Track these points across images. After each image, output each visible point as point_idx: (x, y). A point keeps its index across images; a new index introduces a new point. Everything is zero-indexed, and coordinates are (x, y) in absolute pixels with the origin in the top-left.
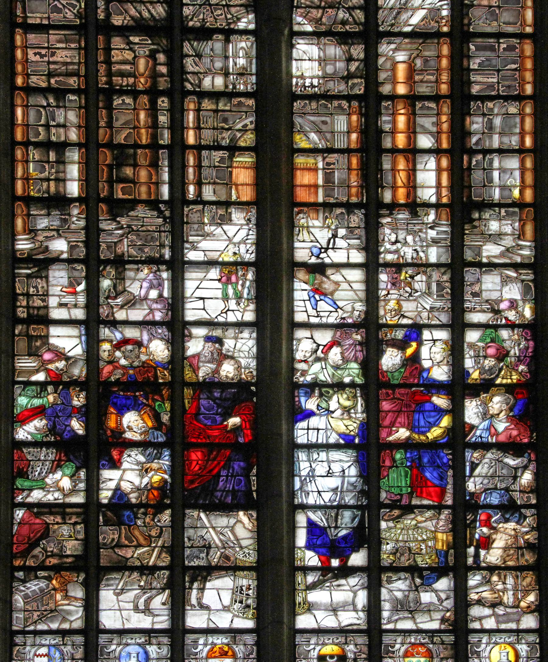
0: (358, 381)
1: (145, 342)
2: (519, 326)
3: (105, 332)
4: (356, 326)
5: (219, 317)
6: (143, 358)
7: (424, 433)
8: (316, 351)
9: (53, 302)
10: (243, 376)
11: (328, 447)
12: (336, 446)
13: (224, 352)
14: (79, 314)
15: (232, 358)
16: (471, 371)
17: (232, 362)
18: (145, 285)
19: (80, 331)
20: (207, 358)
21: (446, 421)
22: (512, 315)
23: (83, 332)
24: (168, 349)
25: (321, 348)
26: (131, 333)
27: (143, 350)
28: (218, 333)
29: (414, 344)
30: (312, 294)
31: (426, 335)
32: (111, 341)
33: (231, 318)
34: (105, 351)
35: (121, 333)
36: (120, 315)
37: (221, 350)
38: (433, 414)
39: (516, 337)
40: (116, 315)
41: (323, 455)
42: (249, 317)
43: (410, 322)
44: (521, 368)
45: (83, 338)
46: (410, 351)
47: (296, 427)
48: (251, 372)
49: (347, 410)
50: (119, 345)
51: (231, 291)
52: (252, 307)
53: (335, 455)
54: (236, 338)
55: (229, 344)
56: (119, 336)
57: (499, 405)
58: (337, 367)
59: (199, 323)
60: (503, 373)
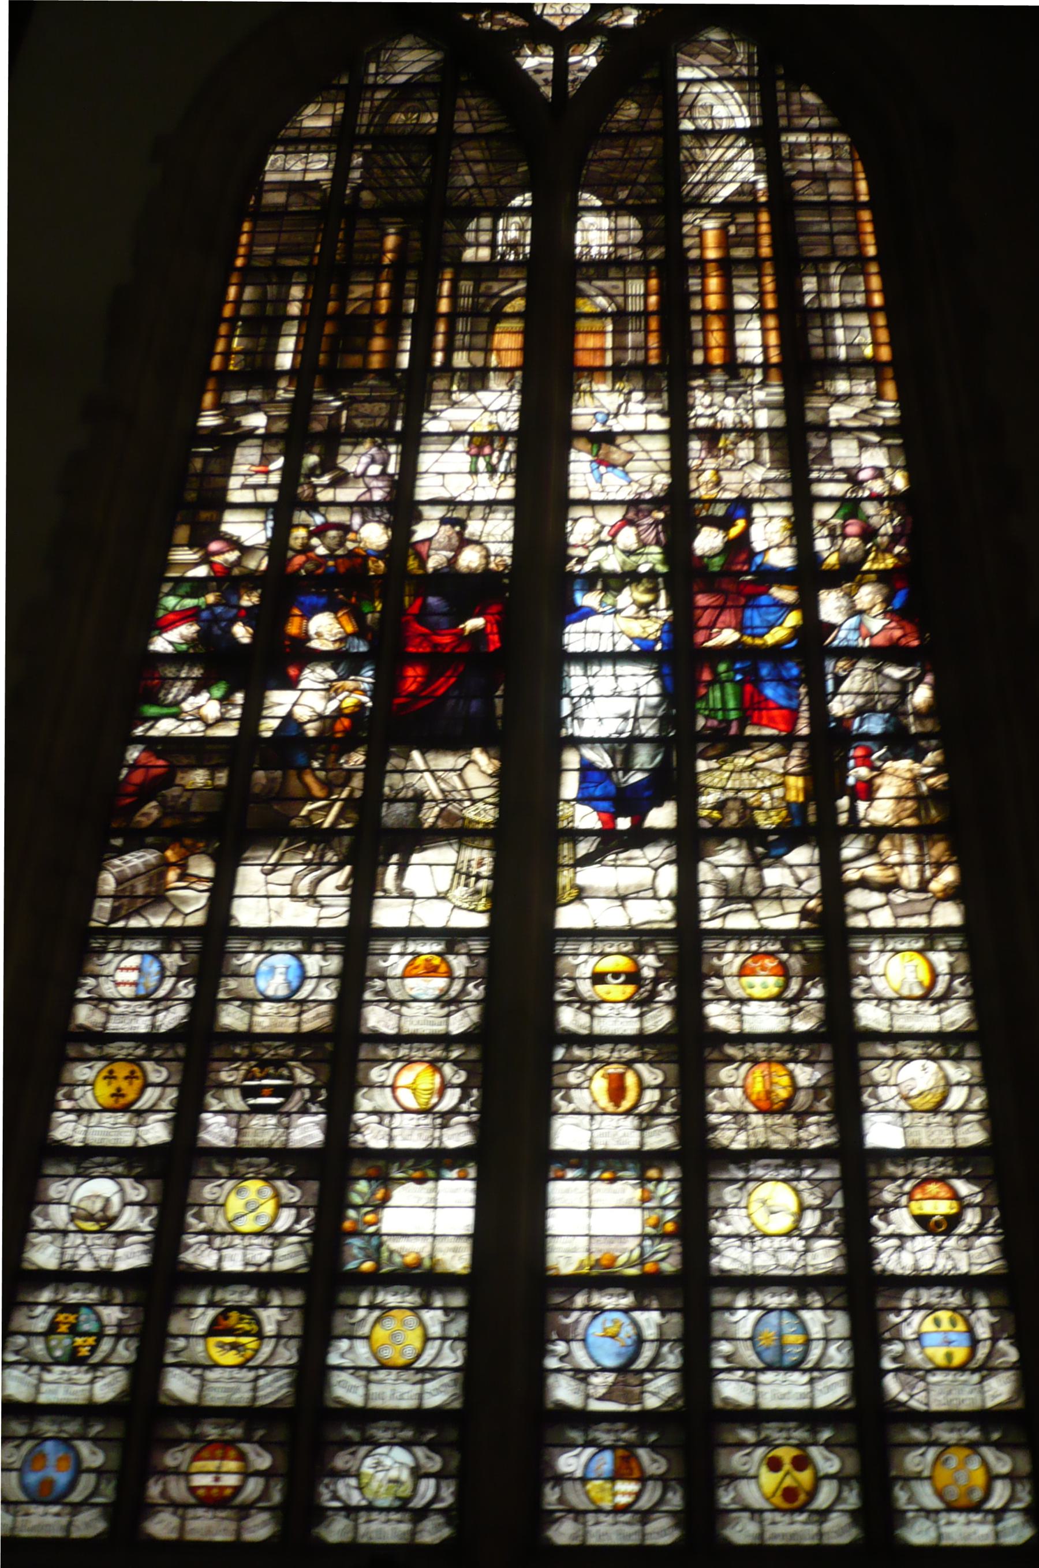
0: (661, 569)
1: (355, 526)
2: (888, 498)
3: (302, 516)
4: (657, 502)
6: (350, 545)
7: (761, 636)
8: (599, 533)
9: (234, 482)
11: (614, 657)
12: (628, 657)
14: (270, 496)
15: (478, 543)
16: (825, 554)
17: (478, 548)
18: (365, 460)
21: (793, 619)
22: (878, 487)
25: (607, 529)
26: (336, 516)
27: (351, 536)
28: (460, 513)
29: (741, 524)
30: (595, 465)
31: (758, 511)
33: (481, 496)
36: (324, 496)
38: (773, 609)
39: (887, 512)
41: (608, 669)
42: (507, 492)
43: (734, 496)
44: (898, 549)
46: (734, 532)
49: (645, 607)
50: (320, 532)
51: (482, 464)
52: (511, 481)
53: (625, 669)
54: (485, 519)
55: (474, 528)
56: (319, 520)
57: (870, 597)
58: (629, 553)
59: (434, 502)
60: (872, 556)
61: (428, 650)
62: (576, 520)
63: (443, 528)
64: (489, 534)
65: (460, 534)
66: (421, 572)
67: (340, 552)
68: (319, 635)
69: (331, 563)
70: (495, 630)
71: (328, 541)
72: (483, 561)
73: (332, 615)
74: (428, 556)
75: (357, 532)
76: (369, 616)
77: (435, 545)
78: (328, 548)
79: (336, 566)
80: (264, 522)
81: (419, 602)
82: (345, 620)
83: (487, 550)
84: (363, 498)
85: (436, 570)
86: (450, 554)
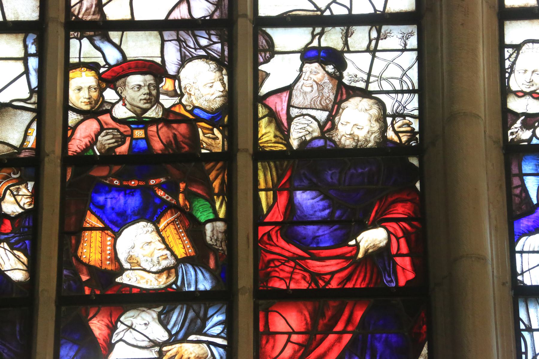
5: (334, 7)
6: (167, 102)
10: (390, 134)
13: (346, 81)
15: (365, 93)
17: (366, 102)
19: (26, 47)
20: (309, 97)
23: (32, 49)
24: (222, 80)
27: (167, 84)
32: (93, 67)
34: (80, 89)
35: (118, 47)
37: (341, 77)
40: (106, 9)
45: (33, 63)
47: (518, 248)
48: (409, 125)
54: (372, 51)
56: (113, 56)
61: (304, 285)
62: (517, 48)
63: (308, 67)
64: (380, 78)
65: (337, 78)
66: (281, 147)
67: (152, 113)
68: (136, 266)
69: (139, 133)
70: (404, 249)
71: (130, 94)
72: (376, 126)
73: (150, 227)
74: (290, 119)
75: (175, 77)
76: (209, 227)
77: (297, 100)
78: (133, 108)
79: (147, 138)
80: (25, 60)
81: (283, 200)
82: (171, 234)
83: (381, 105)
84: (176, 15)
85: (303, 143)
86: (323, 116)
